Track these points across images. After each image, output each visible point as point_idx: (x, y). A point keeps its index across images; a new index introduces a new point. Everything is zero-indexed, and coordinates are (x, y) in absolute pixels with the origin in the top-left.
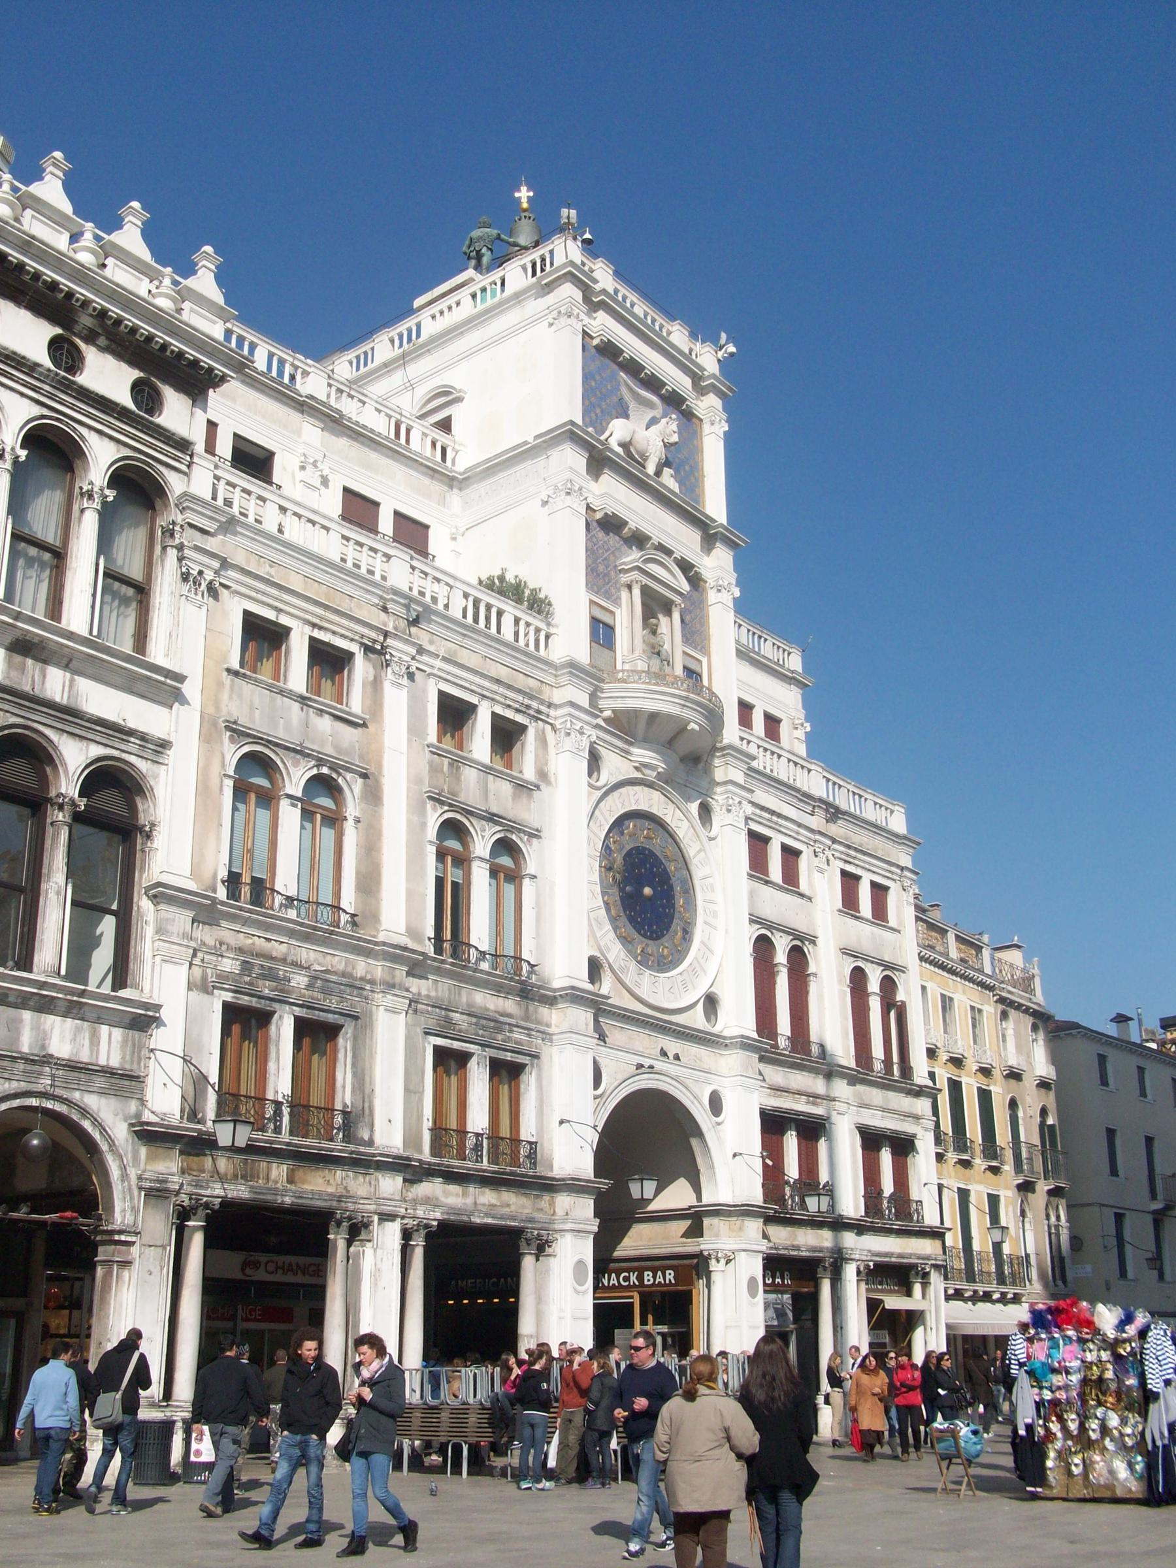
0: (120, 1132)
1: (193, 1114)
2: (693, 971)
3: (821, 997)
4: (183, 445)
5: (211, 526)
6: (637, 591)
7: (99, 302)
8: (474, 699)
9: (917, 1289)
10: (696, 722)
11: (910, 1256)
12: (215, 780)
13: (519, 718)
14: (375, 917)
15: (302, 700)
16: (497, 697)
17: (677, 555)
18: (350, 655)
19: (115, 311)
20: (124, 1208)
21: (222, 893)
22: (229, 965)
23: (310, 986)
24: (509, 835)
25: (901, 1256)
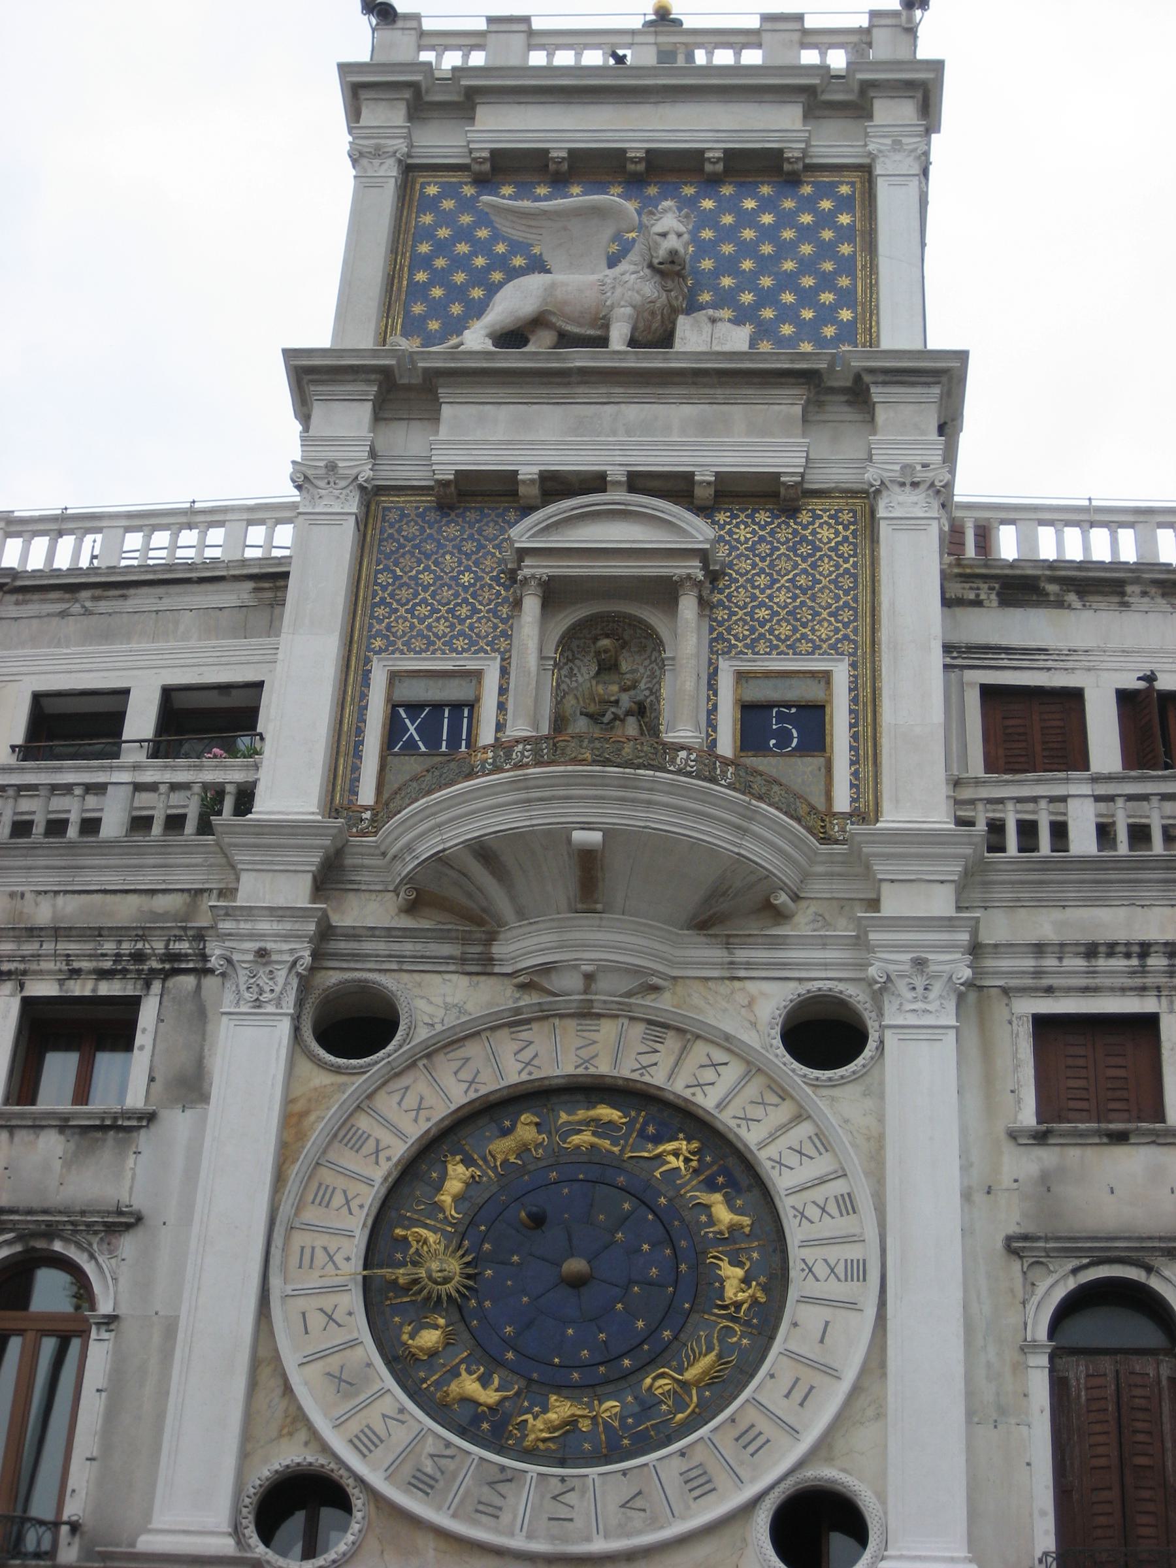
2: (749, 1439)
6: (531, 605)
10: (587, 827)
16: (44, 965)
17: (704, 476)
24: (40, 1244)
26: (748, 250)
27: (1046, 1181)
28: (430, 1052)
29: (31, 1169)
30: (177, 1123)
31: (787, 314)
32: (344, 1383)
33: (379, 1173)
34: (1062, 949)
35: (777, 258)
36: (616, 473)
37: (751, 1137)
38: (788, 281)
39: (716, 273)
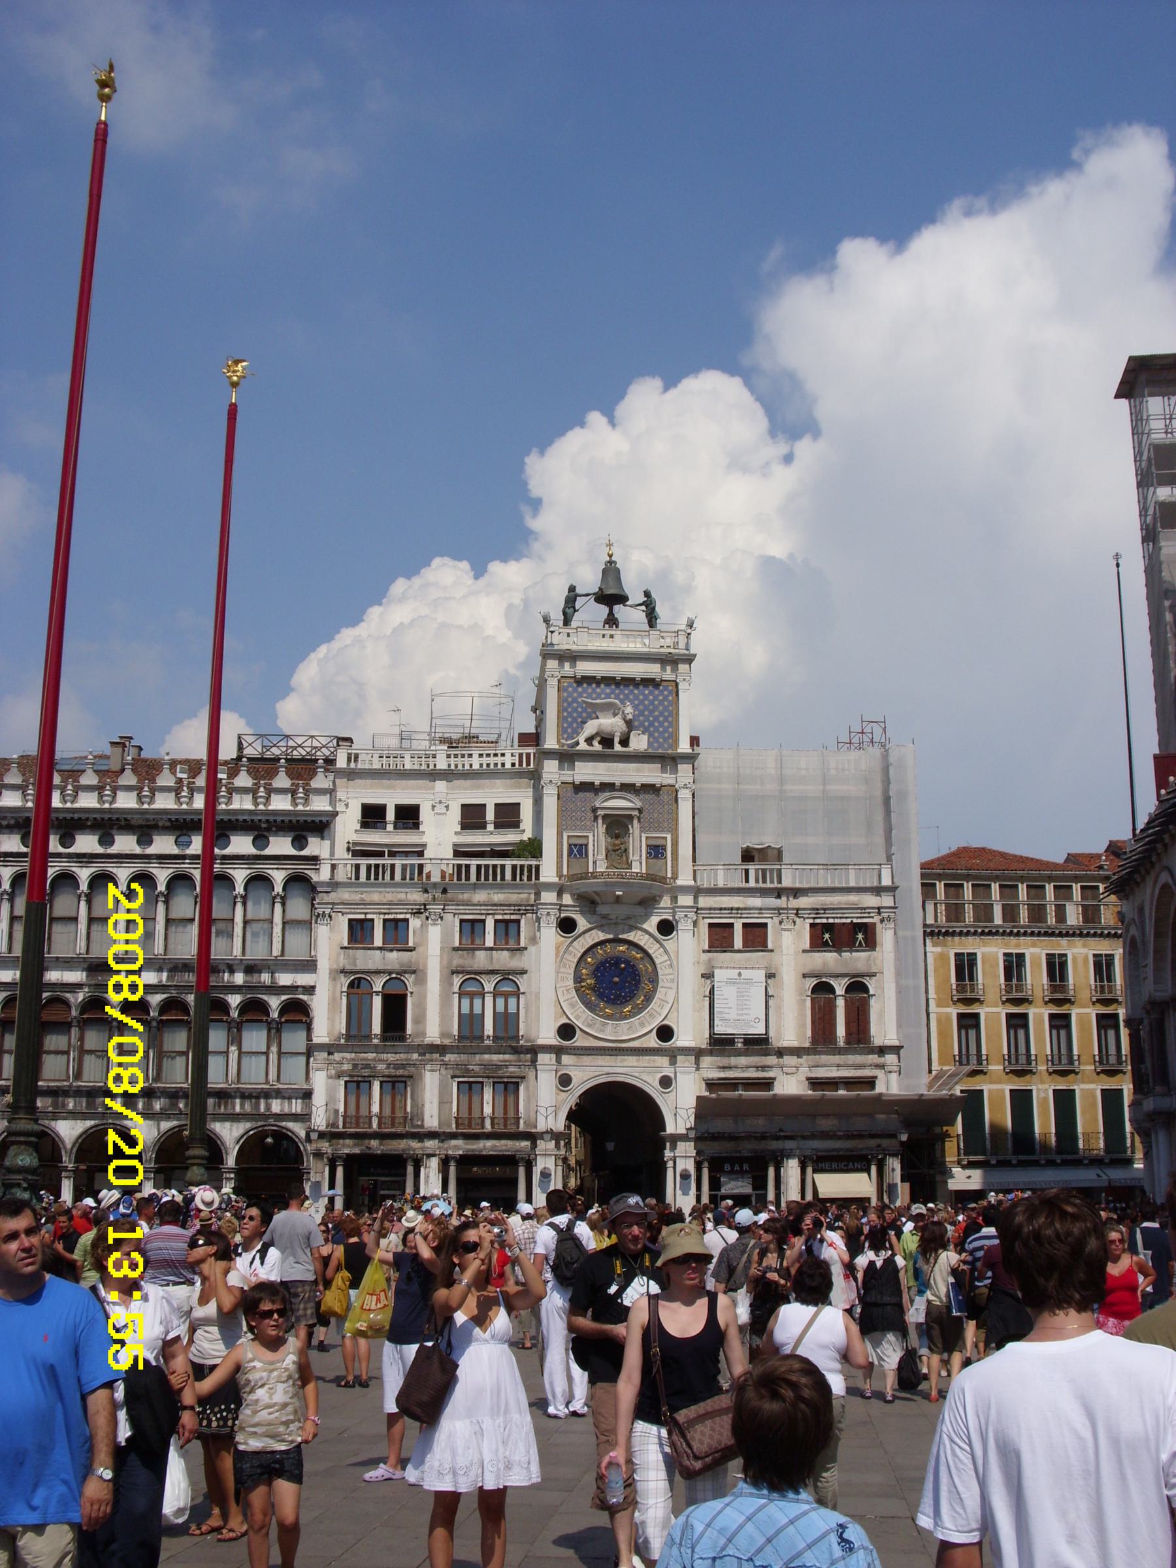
0: (303, 1134)
1: (335, 1125)
3: (779, 1008)
4: (315, 859)
5: (329, 889)
6: (600, 821)
7: (263, 818)
8: (483, 917)
9: (874, 1169)
11: (862, 1149)
12: (338, 993)
13: (513, 917)
14: (424, 1034)
15: (380, 948)
17: (638, 785)
18: (407, 920)
19: (271, 818)
20: (310, 1162)
21: (343, 1041)
22: (346, 1067)
23: (388, 1068)
25: (848, 1150)
26: (646, 708)
27: (710, 961)
28: (584, 933)
29: (503, 959)
30: (532, 949)
31: (656, 730)
32: (572, 1006)
33: (576, 960)
34: (715, 909)
35: (653, 711)
36: (618, 784)
37: (651, 952)
38: (656, 718)
39: (639, 715)
